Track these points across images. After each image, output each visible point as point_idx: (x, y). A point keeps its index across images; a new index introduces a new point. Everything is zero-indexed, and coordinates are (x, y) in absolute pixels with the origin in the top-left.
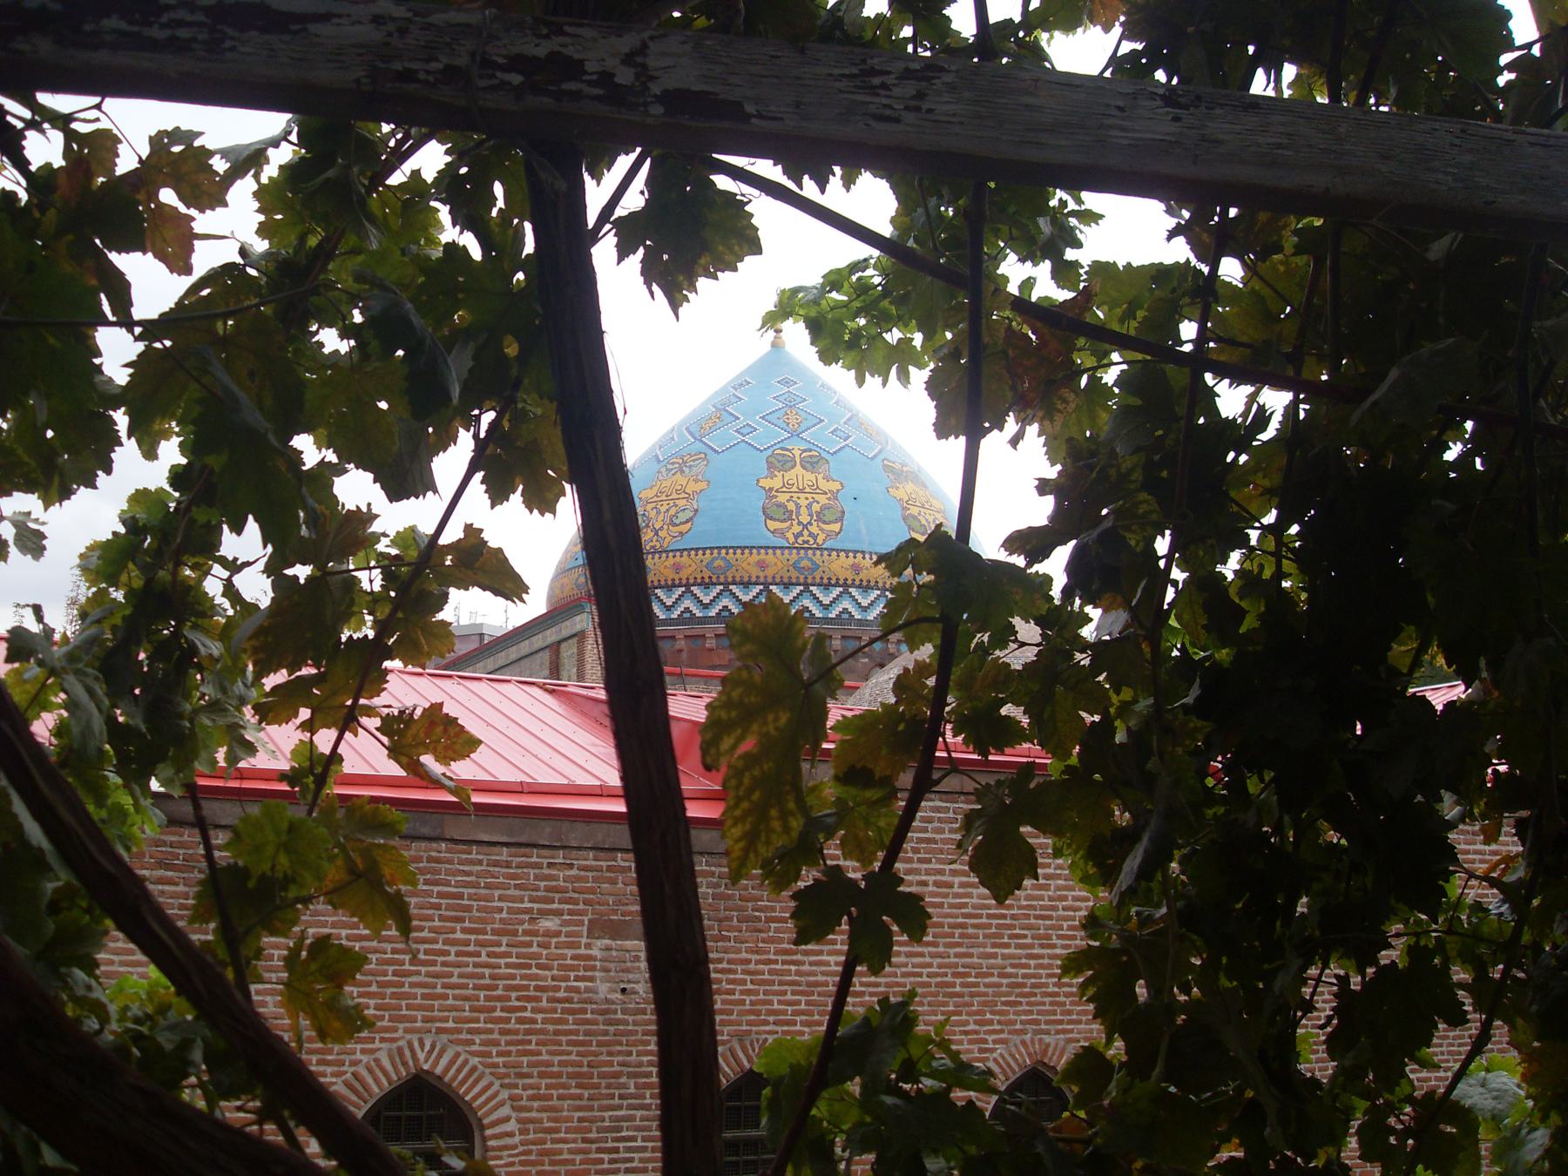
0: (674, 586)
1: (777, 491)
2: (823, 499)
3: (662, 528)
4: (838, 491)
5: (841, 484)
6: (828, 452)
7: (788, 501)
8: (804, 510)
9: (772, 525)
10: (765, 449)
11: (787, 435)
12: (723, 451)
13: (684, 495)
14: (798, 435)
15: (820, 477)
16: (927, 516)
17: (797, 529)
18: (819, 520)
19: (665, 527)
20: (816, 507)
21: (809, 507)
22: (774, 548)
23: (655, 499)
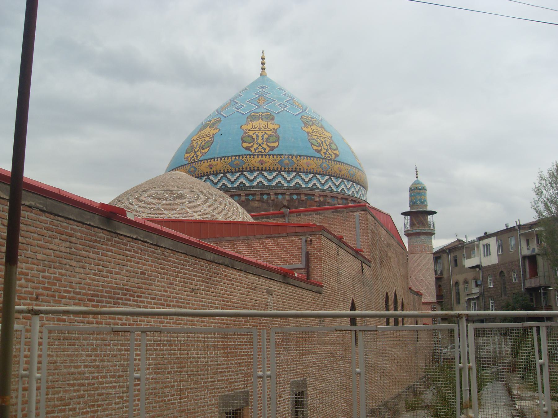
1: (249, 130)
2: (269, 133)
3: (198, 151)
4: (277, 129)
5: (279, 125)
6: (275, 113)
7: (253, 134)
8: (260, 138)
9: (245, 145)
12: (228, 116)
16: (322, 139)
17: (256, 146)
18: (267, 141)
19: (199, 150)
20: (266, 136)
21: (263, 135)
22: (246, 155)
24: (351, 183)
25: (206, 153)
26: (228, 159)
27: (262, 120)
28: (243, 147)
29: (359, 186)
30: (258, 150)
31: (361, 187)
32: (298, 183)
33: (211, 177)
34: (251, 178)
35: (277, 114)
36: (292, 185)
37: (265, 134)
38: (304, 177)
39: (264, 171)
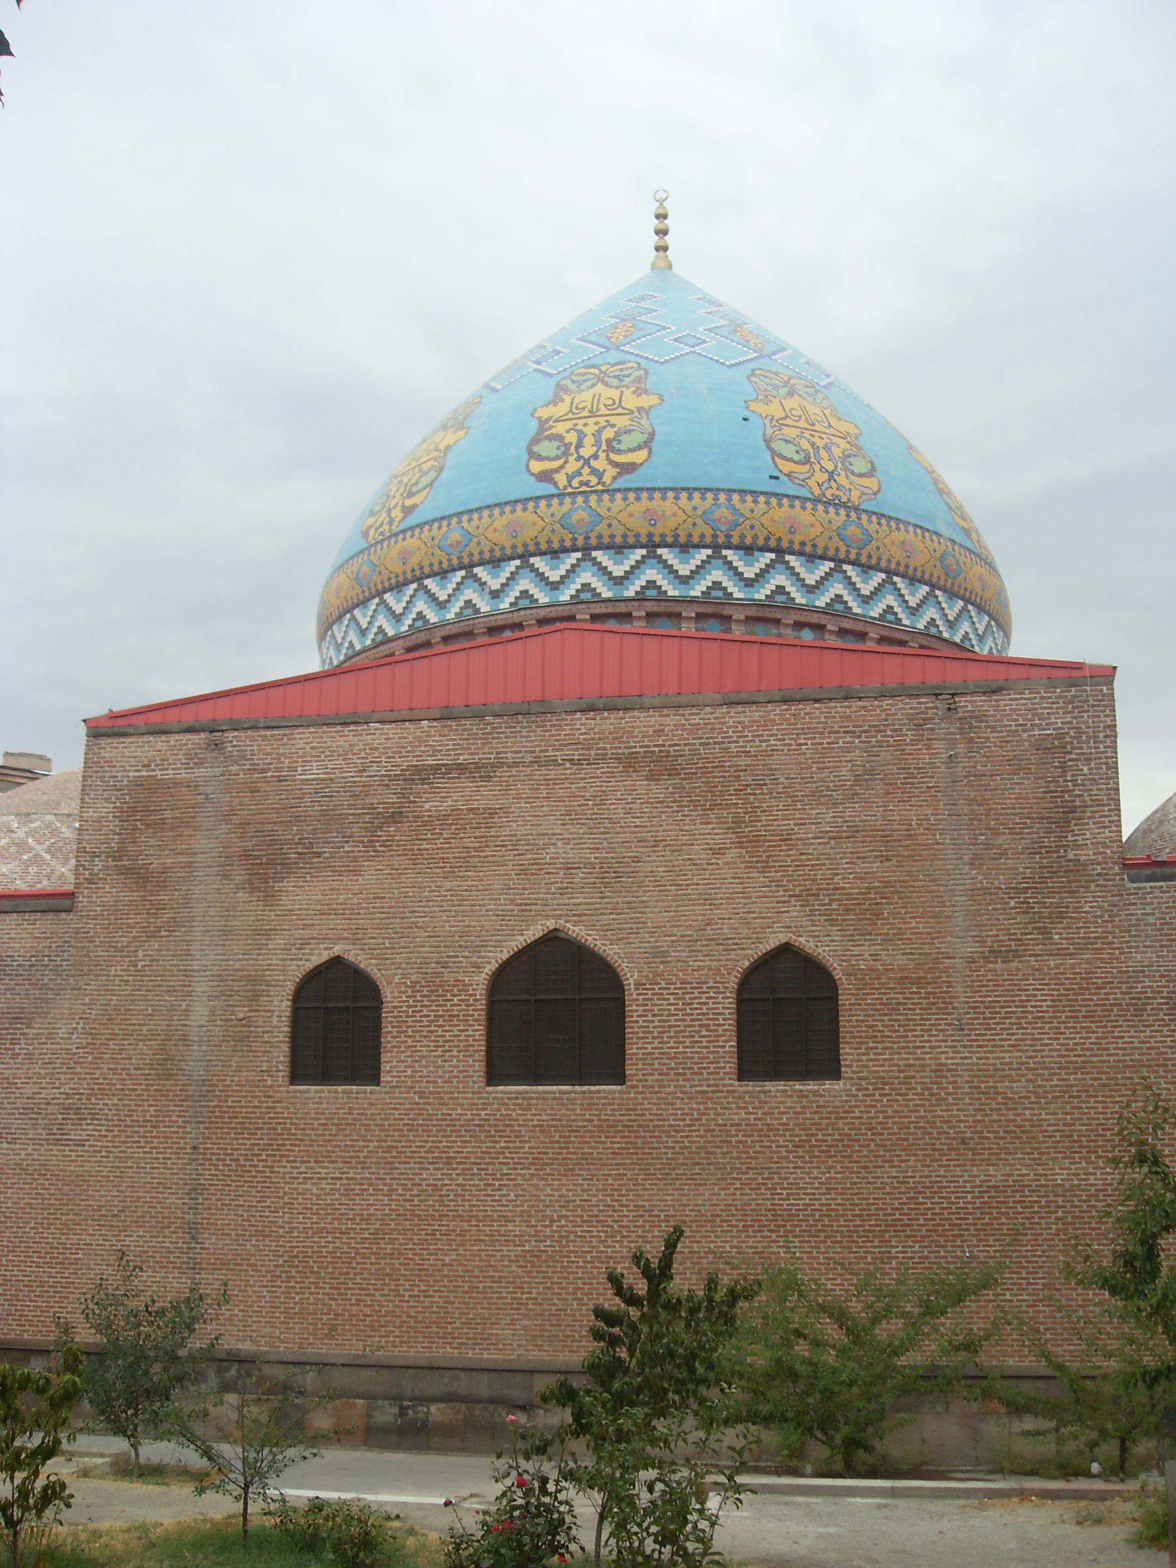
0: (406, 583)
1: (556, 421)
2: (622, 422)
5: (662, 400)
6: (657, 362)
7: (568, 431)
8: (589, 441)
9: (536, 466)
10: (559, 373)
14: (618, 349)
15: (627, 393)
17: (573, 465)
18: (611, 449)
20: (608, 433)
21: (600, 431)
24: (926, 589)
26: (480, 518)
27: (607, 385)
28: (533, 474)
29: (961, 603)
30: (578, 479)
31: (970, 607)
32: (717, 585)
33: (430, 583)
34: (554, 576)
35: (662, 363)
36: (697, 590)
37: (605, 427)
38: (742, 563)
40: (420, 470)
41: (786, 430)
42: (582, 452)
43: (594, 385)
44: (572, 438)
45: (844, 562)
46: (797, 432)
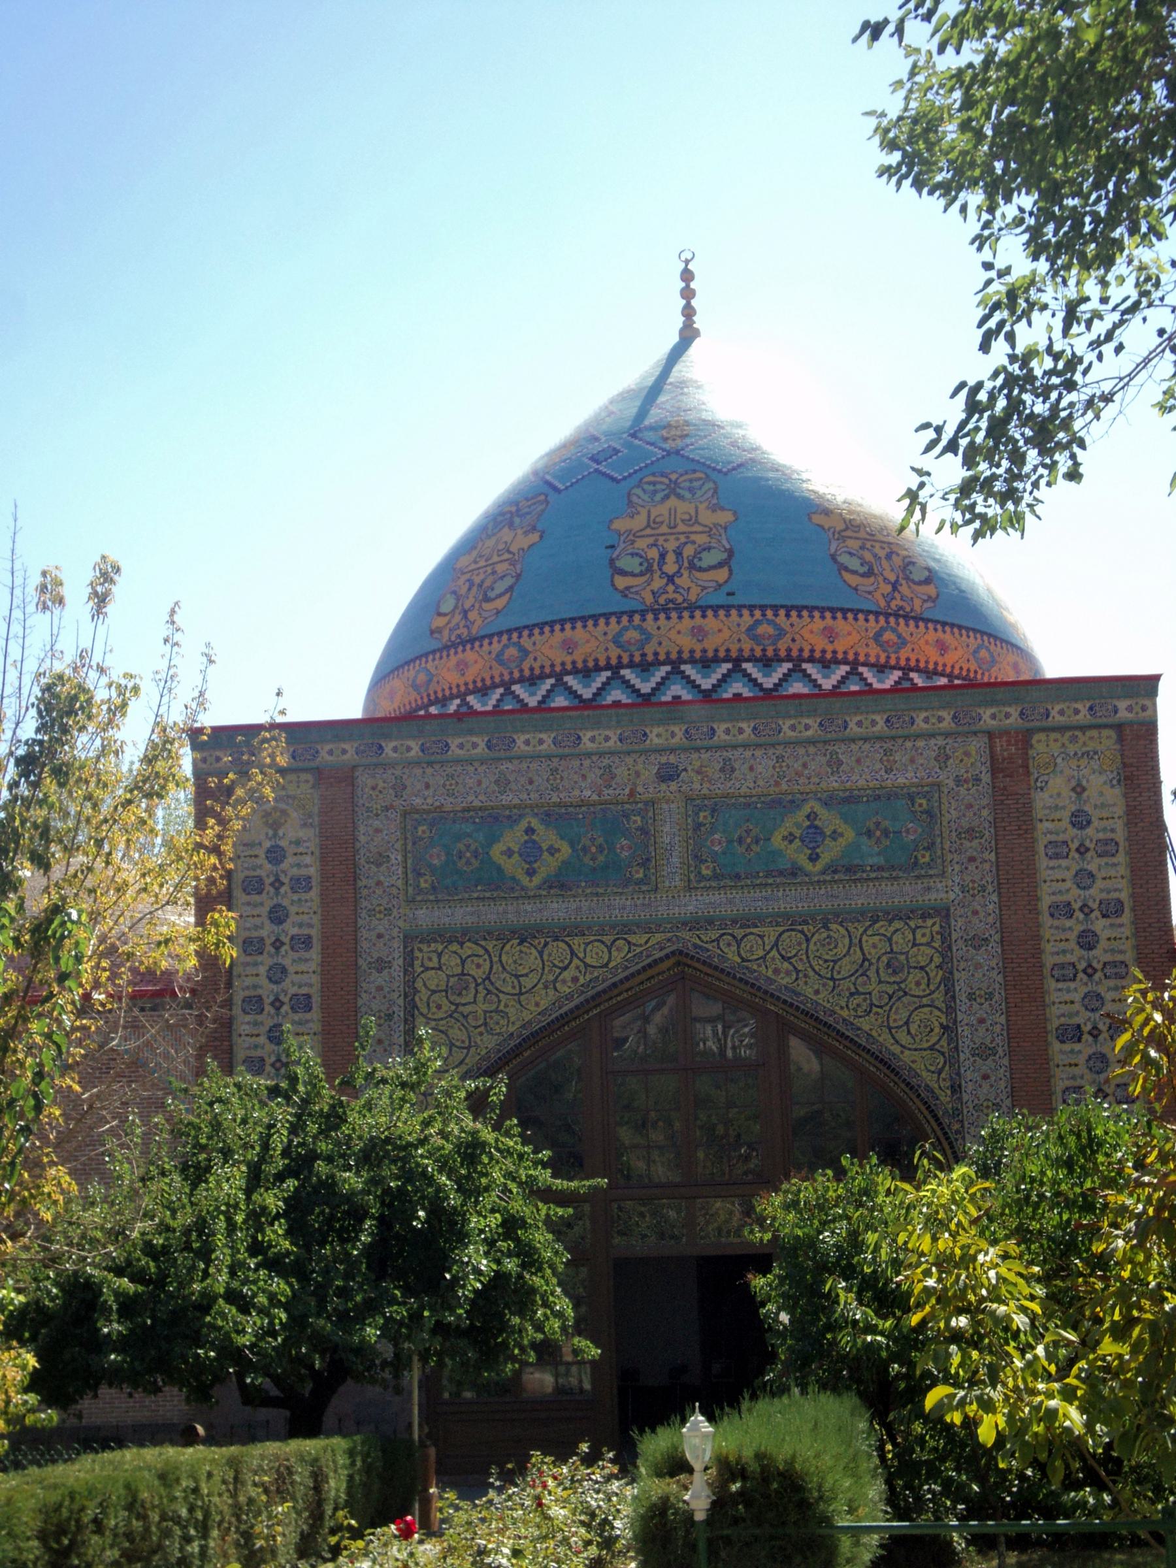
5: (735, 513)
6: (720, 471)
8: (671, 558)
9: (621, 582)
10: (625, 478)
11: (660, 454)
13: (506, 556)
15: (702, 507)
16: (877, 550)
17: (658, 583)
20: (688, 551)
23: (473, 566)
25: (498, 612)
27: (680, 497)
30: (665, 596)
39: (685, 662)
40: (494, 572)
41: (850, 543)
42: (665, 568)
43: (667, 497)
44: (653, 554)
45: (912, 670)
46: (859, 543)
